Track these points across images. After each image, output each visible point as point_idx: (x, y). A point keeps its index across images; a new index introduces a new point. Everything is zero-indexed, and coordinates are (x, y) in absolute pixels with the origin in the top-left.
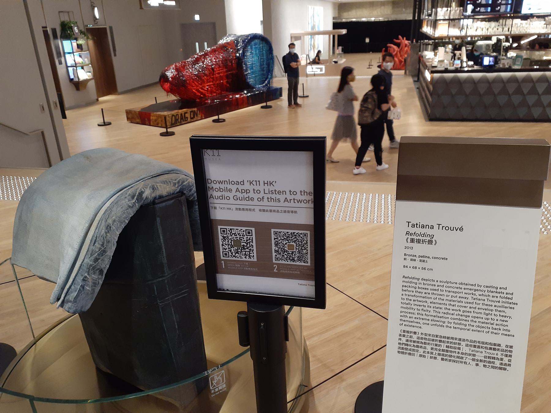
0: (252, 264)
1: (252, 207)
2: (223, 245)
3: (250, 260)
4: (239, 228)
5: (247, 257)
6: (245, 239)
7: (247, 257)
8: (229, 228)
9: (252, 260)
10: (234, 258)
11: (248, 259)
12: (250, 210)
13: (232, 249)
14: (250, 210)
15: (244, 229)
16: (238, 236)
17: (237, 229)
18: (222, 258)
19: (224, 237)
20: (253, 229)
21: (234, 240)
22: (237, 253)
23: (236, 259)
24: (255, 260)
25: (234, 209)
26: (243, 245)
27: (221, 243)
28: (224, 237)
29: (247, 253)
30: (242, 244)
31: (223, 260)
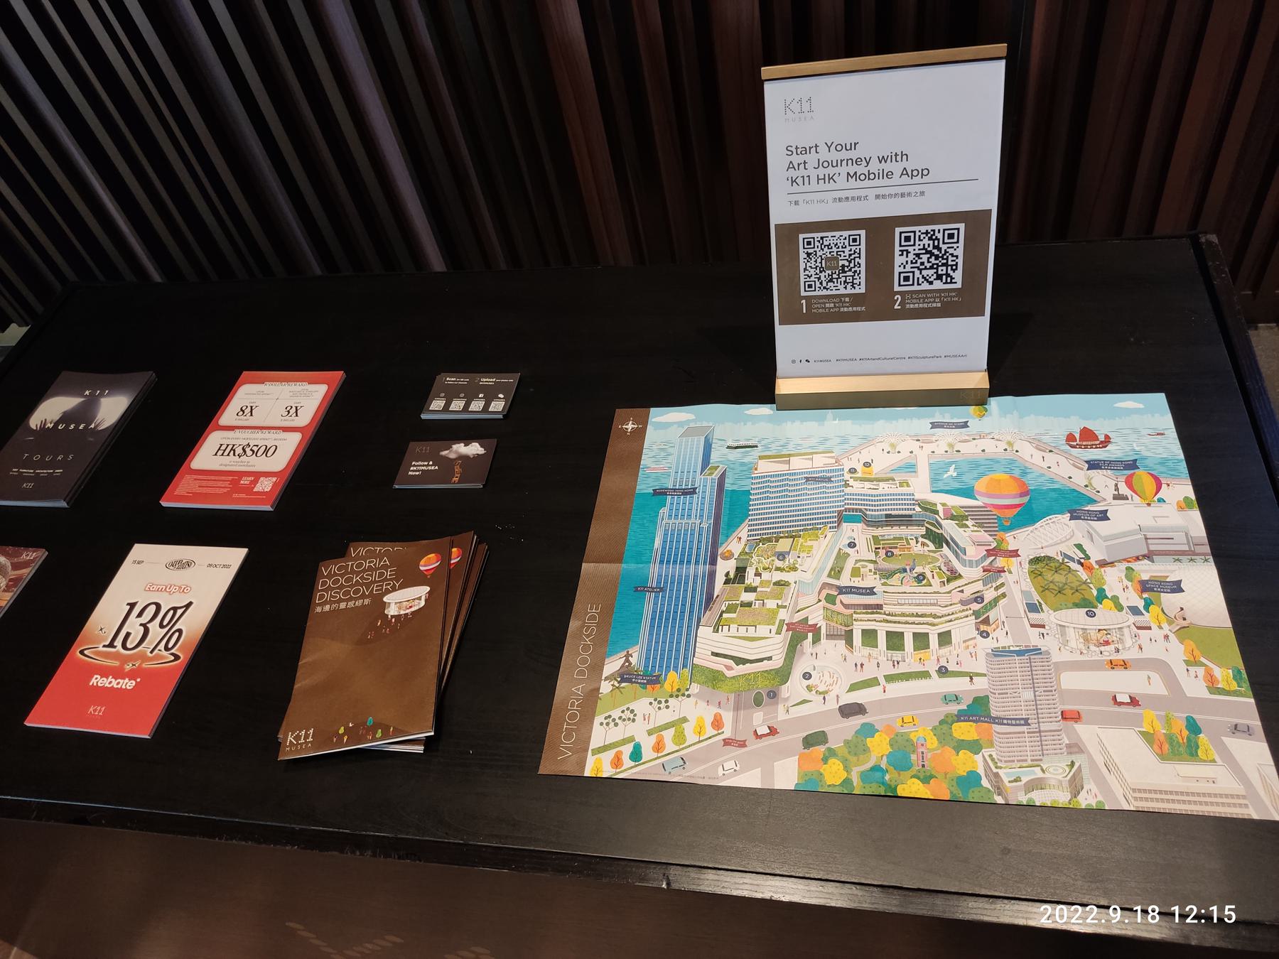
0: (856, 299)
1: (862, 193)
2: (805, 269)
3: (853, 291)
4: (837, 234)
5: (849, 286)
6: (847, 253)
7: (849, 286)
8: (818, 235)
9: (857, 291)
10: (825, 292)
11: (849, 291)
12: (859, 198)
13: (822, 275)
14: (859, 198)
15: (845, 234)
16: (834, 249)
17: (832, 237)
18: (803, 293)
19: (809, 255)
20: (863, 233)
21: (827, 259)
22: (831, 281)
23: (829, 293)
24: (863, 291)
25: (830, 201)
26: (843, 266)
27: (802, 266)
28: (809, 255)
29: (849, 279)
30: (841, 263)
31: (805, 297)
